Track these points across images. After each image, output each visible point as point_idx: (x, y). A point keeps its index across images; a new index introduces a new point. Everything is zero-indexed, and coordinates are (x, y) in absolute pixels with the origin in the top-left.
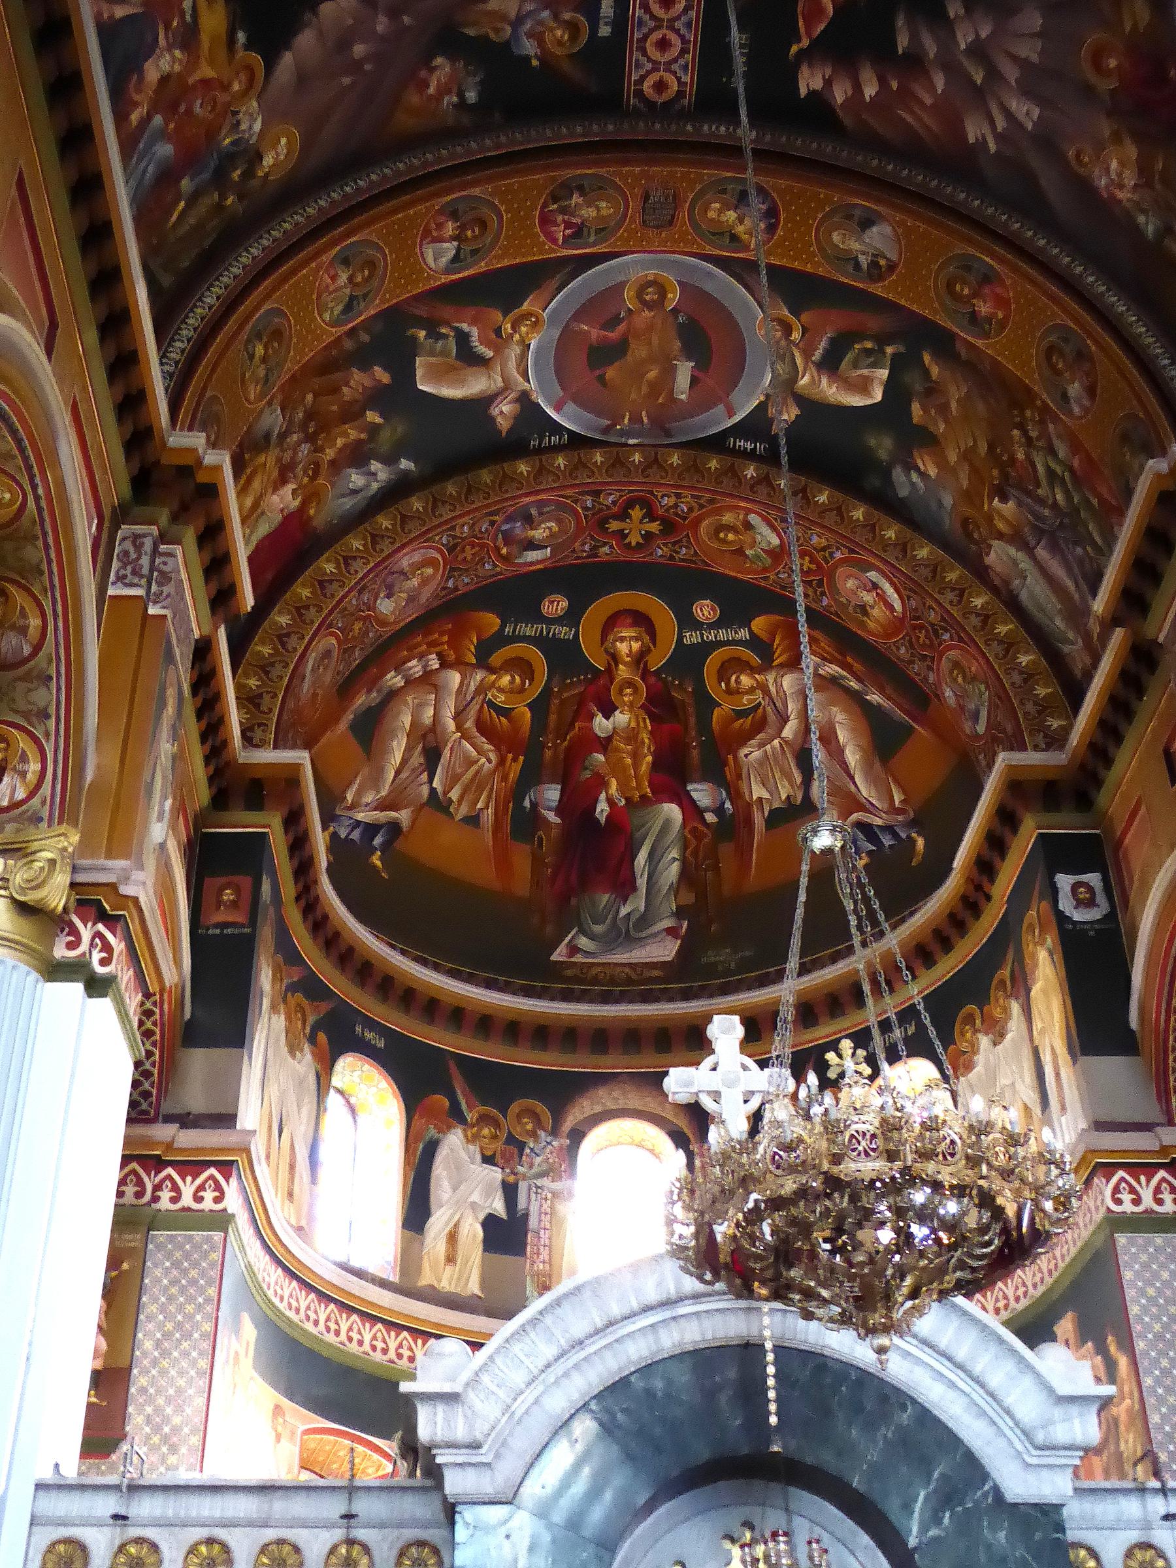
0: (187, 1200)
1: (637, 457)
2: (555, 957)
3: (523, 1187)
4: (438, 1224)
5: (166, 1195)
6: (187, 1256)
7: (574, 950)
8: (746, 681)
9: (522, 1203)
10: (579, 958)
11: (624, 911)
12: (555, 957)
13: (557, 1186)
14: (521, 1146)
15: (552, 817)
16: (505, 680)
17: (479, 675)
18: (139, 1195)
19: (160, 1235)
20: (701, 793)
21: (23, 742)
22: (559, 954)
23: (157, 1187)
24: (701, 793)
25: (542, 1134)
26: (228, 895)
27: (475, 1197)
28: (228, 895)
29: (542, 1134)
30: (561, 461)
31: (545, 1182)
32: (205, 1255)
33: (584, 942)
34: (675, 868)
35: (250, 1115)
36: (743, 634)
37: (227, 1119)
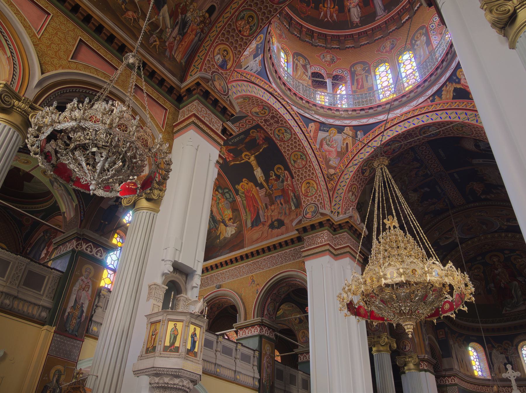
0: (450, 382)
1: (482, 238)
2: (503, 313)
3: (509, 357)
4: (496, 366)
5: (447, 381)
6: (453, 390)
7: (506, 311)
8: (519, 260)
9: (510, 360)
10: (508, 312)
11: (513, 302)
12: (503, 313)
13: (516, 355)
14: (507, 350)
15: (493, 289)
16: (476, 271)
17: (471, 272)
18: (443, 382)
19: (448, 388)
20: (520, 279)
21: (407, 342)
22: (504, 312)
23: (446, 380)
24: (520, 279)
25: (510, 347)
26: (441, 333)
27: (501, 360)
28: (441, 333)
29: (510, 347)
30: (470, 242)
31: (513, 355)
32: (455, 390)
33: (508, 309)
34: (520, 292)
35: (456, 367)
36: (515, 254)
37: (451, 369)
